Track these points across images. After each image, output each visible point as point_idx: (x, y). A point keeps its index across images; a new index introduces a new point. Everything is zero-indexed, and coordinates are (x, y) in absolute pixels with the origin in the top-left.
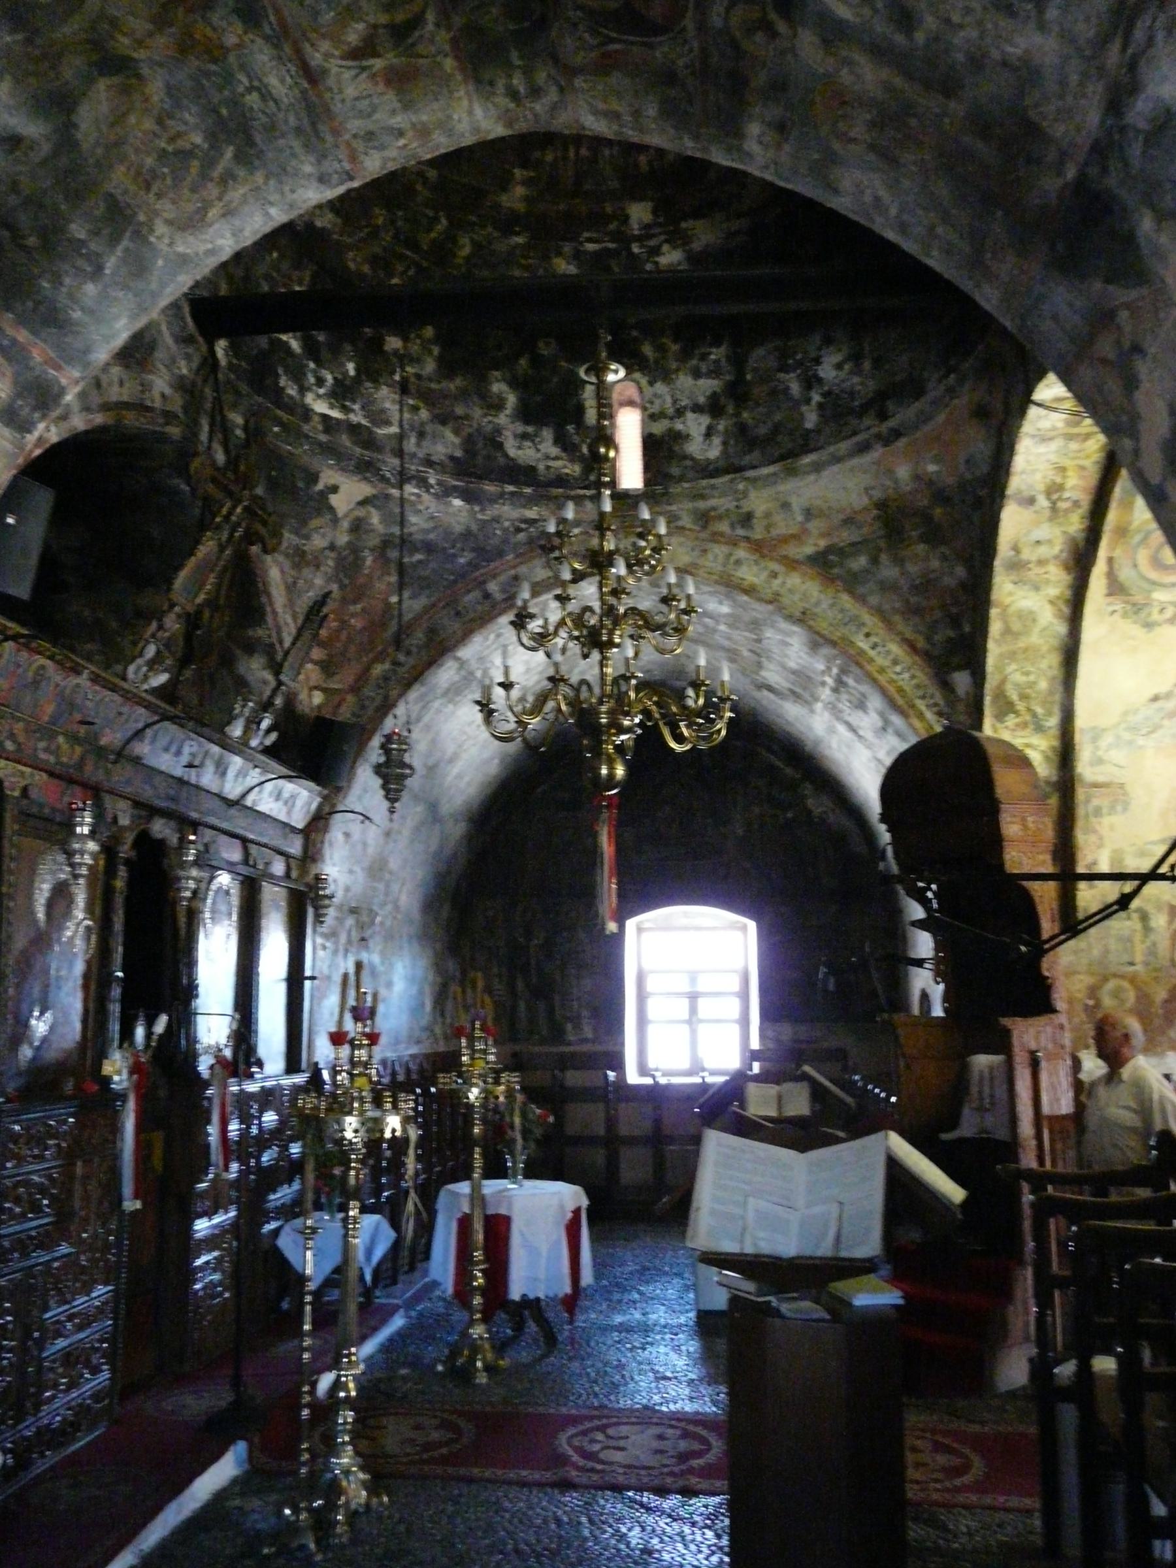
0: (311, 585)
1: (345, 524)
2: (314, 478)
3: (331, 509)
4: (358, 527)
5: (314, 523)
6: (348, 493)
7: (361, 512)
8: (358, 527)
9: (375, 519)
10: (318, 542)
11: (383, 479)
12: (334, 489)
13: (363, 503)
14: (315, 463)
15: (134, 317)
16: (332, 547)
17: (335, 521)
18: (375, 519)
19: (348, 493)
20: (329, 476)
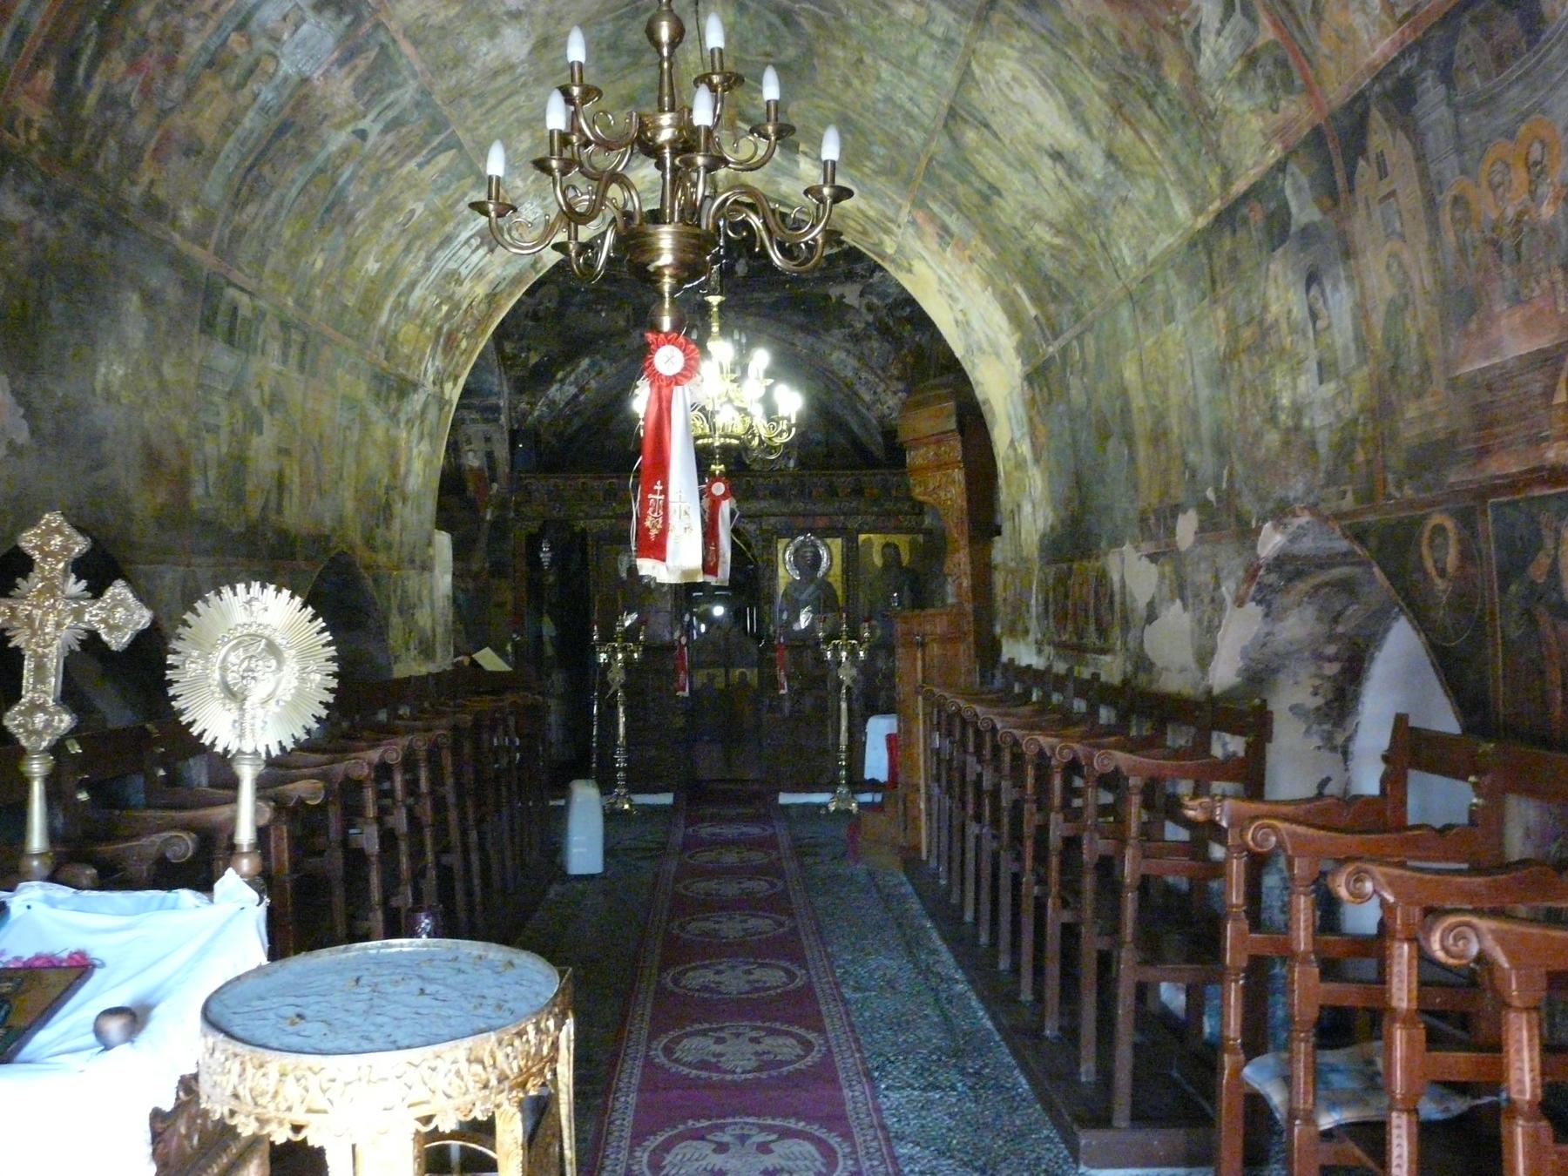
0: (872, 350)
1: (864, 310)
2: (827, 297)
3: (851, 307)
4: (870, 308)
5: (848, 318)
6: (850, 294)
7: (865, 301)
8: (870, 308)
9: (875, 301)
10: (859, 326)
11: (863, 277)
12: (842, 296)
13: (862, 295)
14: (819, 290)
15: (492, 374)
16: (868, 324)
17: (858, 311)
18: (875, 301)
19: (850, 294)
20: (834, 291)
